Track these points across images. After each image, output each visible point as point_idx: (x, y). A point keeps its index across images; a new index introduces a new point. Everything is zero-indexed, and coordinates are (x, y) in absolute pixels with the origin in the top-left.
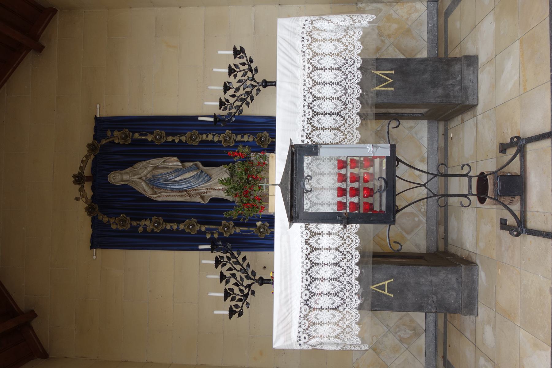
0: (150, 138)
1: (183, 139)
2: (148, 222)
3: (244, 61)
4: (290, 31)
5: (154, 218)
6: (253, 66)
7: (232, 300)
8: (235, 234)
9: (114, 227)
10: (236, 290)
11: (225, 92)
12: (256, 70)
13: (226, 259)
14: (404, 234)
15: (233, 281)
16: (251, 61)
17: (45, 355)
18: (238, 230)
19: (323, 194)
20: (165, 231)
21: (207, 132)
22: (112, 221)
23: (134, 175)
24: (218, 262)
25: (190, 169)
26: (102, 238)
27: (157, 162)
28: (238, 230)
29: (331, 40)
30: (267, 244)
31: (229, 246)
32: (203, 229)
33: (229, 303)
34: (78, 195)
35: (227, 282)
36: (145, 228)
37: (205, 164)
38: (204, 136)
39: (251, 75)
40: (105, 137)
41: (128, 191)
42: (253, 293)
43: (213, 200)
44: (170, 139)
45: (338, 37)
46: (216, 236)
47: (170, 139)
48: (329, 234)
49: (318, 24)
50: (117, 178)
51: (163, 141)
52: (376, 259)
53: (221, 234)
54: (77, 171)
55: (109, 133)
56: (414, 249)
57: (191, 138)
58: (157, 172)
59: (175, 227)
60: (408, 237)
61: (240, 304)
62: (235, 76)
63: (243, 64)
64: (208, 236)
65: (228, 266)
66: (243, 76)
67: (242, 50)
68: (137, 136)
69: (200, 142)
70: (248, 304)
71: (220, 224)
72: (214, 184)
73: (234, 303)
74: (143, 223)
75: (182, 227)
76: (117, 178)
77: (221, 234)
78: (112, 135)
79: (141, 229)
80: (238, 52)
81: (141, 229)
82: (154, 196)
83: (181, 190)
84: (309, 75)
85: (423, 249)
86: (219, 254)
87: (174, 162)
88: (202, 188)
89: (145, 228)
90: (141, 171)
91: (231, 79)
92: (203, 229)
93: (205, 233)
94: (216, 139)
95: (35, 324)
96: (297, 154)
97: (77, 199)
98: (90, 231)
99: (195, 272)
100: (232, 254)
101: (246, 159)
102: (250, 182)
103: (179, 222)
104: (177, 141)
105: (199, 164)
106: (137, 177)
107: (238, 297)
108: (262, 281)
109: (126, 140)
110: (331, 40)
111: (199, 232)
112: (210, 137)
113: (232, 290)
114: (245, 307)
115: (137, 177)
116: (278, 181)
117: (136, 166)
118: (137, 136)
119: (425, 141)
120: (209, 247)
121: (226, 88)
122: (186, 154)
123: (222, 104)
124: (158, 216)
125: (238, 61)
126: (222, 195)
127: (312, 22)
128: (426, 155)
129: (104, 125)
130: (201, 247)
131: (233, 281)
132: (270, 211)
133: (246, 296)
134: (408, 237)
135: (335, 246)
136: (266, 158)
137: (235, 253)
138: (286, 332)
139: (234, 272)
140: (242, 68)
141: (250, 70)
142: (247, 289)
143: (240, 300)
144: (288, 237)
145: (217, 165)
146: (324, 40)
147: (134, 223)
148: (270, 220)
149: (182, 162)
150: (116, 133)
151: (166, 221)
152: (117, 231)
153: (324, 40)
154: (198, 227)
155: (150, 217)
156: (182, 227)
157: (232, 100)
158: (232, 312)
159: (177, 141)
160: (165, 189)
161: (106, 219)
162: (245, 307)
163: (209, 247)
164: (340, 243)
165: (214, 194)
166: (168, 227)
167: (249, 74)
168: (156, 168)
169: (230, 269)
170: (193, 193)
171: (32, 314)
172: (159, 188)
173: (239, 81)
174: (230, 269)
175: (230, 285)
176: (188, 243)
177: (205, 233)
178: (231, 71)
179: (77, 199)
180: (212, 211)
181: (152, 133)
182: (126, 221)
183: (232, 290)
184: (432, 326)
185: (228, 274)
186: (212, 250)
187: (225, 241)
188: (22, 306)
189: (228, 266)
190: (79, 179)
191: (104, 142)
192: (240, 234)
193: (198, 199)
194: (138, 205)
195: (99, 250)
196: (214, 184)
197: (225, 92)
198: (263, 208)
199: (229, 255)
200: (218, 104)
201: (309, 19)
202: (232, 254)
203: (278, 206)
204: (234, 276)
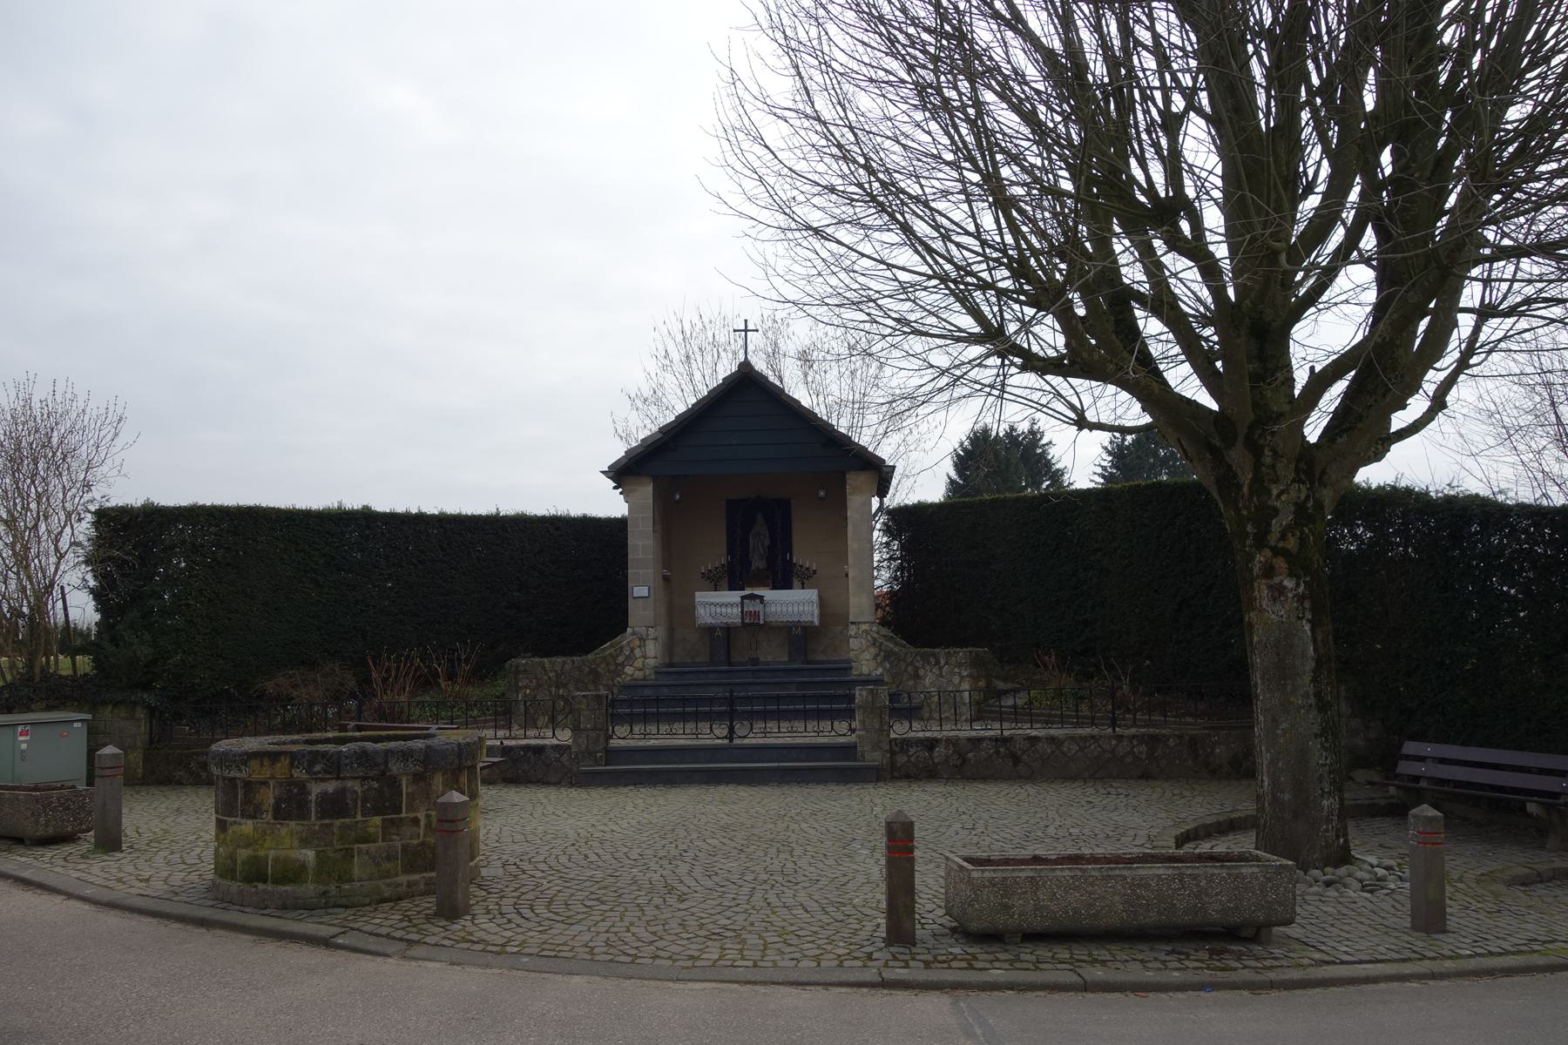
4: (811, 595)
19: (751, 607)
39: (806, 578)
48: (737, 611)
52: (728, 630)
72: (758, 563)
87: (767, 542)
96: (761, 598)
99: (717, 556)
138: (701, 597)
142: (714, 582)
144: (735, 596)
164: (733, 615)
176: (730, 551)
196: (758, 563)
203: (747, 592)
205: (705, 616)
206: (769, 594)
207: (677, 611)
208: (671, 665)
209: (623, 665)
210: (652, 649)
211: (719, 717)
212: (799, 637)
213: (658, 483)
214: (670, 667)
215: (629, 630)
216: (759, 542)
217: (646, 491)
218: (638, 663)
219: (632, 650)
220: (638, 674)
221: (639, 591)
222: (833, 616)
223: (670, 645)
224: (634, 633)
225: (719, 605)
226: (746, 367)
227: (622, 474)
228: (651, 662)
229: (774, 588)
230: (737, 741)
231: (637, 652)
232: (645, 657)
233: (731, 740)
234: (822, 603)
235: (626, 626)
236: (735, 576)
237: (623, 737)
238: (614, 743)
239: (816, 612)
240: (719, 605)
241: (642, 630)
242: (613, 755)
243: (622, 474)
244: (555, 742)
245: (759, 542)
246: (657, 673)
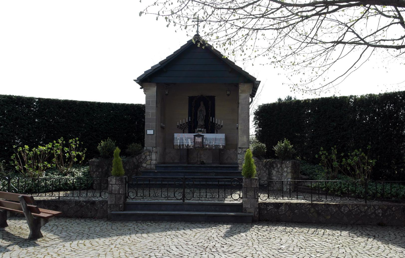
26: (191, 99)
27: (205, 110)
30: (190, 132)
50: (202, 103)
72: (201, 123)
76: (202, 103)
87: (205, 114)
99: (184, 118)
106: (202, 107)
108: (183, 131)
115: (202, 107)
129: (212, 99)
138: (176, 135)
142: (182, 129)
144: (192, 135)
182: (194, 104)
192: (191, 128)
196: (201, 123)
205: (177, 142)
207: (167, 141)
208: (164, 163)
209: (141, 163)
210: (154, 156)
211: (180, 186)
212: (218, 153)
214: (163, 165)
216: (202, 113)
217: (153, 90)
218: (148, 162)
219: (146, 157)
220: (148, 167)
221: (150, 132)
222: (231, 144)
223: (163, 155)
225: (185, 139)
226: (197, 36)
227: (144, 81)
228: (154, 162)
230: (186, 201)
231: (148, 158)
232: (151, 160)
233: (184, 201)
237: (135, 197)
238: (129, 201)
240: (185, 139)
242: (127, 206)
243: (144, 81)
244: (100, 199)
245: (202, 113)
246: (156, 167)
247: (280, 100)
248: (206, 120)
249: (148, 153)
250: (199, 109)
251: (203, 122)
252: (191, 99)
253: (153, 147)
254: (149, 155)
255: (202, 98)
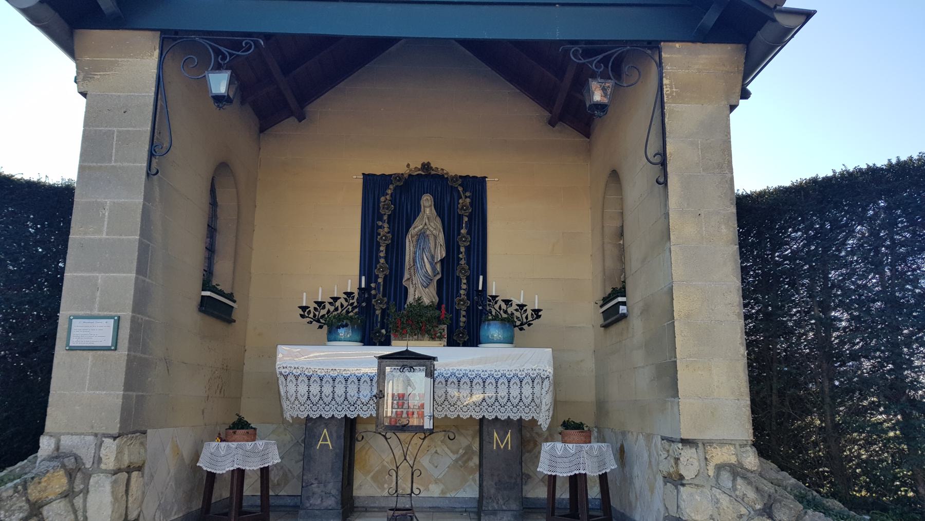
0: (463, 231)
1: (463, 262)
2: (386, 230)
3: (530, 318)
5: (390, 235)
6: (525, 327)
7: (315, 309)
8: (375, 310)
9: (382, 199)
10: (323, 312)
11: (503, 301)
12: (521, 329)
13: (351, 301)
14: (372, 474)
15: (332, 309)
16: (529, 325)
17: (262, 130)
18: (378, 312)
20: (379, 245)
21: (468, 283)
22: (388, 197)
23: (428, 218)
24: (349, 294)
25: (434, 269)
26: (373, 185)
28: (378, 312)
29: (533, 394)
31: (364, 304)
32: (380, 280)
33: (312, 306)
34: (412, 167)
35: (330, 303)
36: (381, 227)
37: (439, 282)
38: (465, 281)
39: (518, 323)
40: (465, 191)
41: (416, 211)
42: (321, 327)
43: (406, 289)
44: (463, 249)
45: (535, 399)
46: (373, 292)
47: (463, 249)
49: (546, 382)
50: (427, 201)
51: (460, 243)
53: (375, 296)
54: (433, 165)
55: (468, 194)
56: (356, 484)
57: (463, 269)
58: (432, 239)
59: (382, 254)
60: (369, 478)
61: (311, 315)
62: (517, 310)
63: (527, 318)
64: (373, 285)
65: (345, 304)
66: (517, 318)
67: (539, 317)
68: (466, 219)
69: (458, 277)
70: (311, 322)
71: (384, 296)
72: (421, 291)
73: (312, 310)
74: (386, 225)
75: (382, 261)
76: (427, 201)
77: (375, 296)
78: (466, 197)
79: (380, 223)
80: (537, 313)
81: (380, 223)
82: (409, 237)
83: (414, 261)
84: (503, 375)
85: (356, 493)
86: (356, 296)
87: (440, 253)
88: (418, 279)
89: (381, 227)
90: (432, 224)
91: (515, 307)
92: (380, 280)
93: (376, 282)
94: (462, 292)
95: (292, 120)
96: (427, 361)
97: (408, 165)
98: (378, 174)
100: (356, 307)
101: (440, 322)
102: (421, 323)
103: (386, 258)
104: (461, 256)
105: (439, 277)
106: (428, 219)
107: (317, 313)
109: (464, 206)
110: (533, 394)
111: (377, 277)
112: (464, 287)
113: (324, 308)
114: (309, 320)
115: (428, 219)
116: (410, 349)
117: (438, 219)
118: (466, 219)
119: (461, 494)
120: (363, 286)
121: (507, 302)
122: (448, 263)
123: (494, 297)
124: (392, 239)
125: (529, 312)
126: (410, 299)
127: (548, 377)
128: (448, 496)
129: (476, 187)
130: (363, 278)
131: (332, 309)
132: (393, 342)
133: (318, 321)
134: (369, 478)
135: (361, 397)
136: (441, 338)
137: (357, 310)
139: (340, 309)
140: (524, 316)
141: (522, 324)
143: (315, 315)
145: (439, 292)
146: (533, 387)
147: (385, 218)
148: (387, 343)
149: (442, 261)
150: (468, 200)
151: (387, 246)
152: (379, 202)
153: (533, 387)
154: (381, 275)
155: (391, 231)
156: (382, 261)
157: (497, 307)
158: (304, 308)
159: (461, 256)
160: (415, 247)
161: (389, 192)
162: (309, 320)
163: (363, 286)
165: (411, 291)
166: (382, 248)
167: (518, 323)
168: (435, 237)
169: (342, 305)
170: (412, 271)
171: (301, 118)
172: (417, 241)
173: (512, 314)
174: (342, 305)
175: (328, 306)
176: (367, 266)
177: (376, 282)
178: (521, 306)
179: (408, 165)
180: (395, 287)
181: (468, 233)
183: (324, 308)
184: (281, 502)
185: (338, 304)
186: (360, 288)
187: (368, 301)
188: (310, 108)
189: (345, 304)
190: (426, 166)
191: (460, 189)
193: (406, 276)
194: (403, 218)
195: (361, 181)
197: (503, 301)
198: (396, 336)
199: (355, 304)
200: (494, 294)
201: (551, 375)
202: (356, 307)
204: (336, 309)
206: (451, 359)
213: (172, 41)
215: (46, 444)
221: (99, 332)
224: (58, 455)
229: (451, 343)
234: (557, 383)
235: (40, 429)
236: (374, 314)
239: (547, 400)
241: (83, 446)
247: (834, 171)
248: (446, 284)
249: (59, 482)
250: (413, 231)
251: (433, 290)
252: (373, 185)
253: (100, 437)
254: (68, 495)
255: (427, 180)
